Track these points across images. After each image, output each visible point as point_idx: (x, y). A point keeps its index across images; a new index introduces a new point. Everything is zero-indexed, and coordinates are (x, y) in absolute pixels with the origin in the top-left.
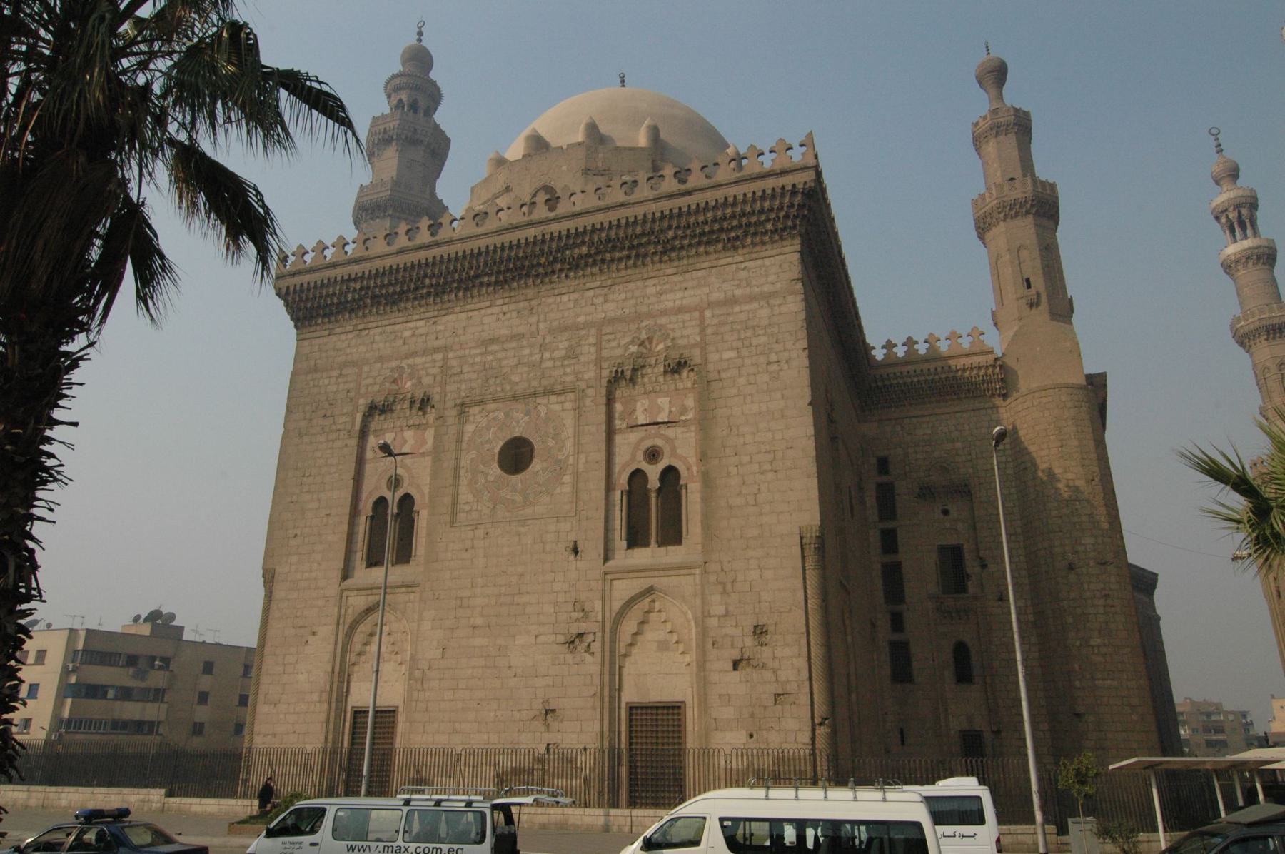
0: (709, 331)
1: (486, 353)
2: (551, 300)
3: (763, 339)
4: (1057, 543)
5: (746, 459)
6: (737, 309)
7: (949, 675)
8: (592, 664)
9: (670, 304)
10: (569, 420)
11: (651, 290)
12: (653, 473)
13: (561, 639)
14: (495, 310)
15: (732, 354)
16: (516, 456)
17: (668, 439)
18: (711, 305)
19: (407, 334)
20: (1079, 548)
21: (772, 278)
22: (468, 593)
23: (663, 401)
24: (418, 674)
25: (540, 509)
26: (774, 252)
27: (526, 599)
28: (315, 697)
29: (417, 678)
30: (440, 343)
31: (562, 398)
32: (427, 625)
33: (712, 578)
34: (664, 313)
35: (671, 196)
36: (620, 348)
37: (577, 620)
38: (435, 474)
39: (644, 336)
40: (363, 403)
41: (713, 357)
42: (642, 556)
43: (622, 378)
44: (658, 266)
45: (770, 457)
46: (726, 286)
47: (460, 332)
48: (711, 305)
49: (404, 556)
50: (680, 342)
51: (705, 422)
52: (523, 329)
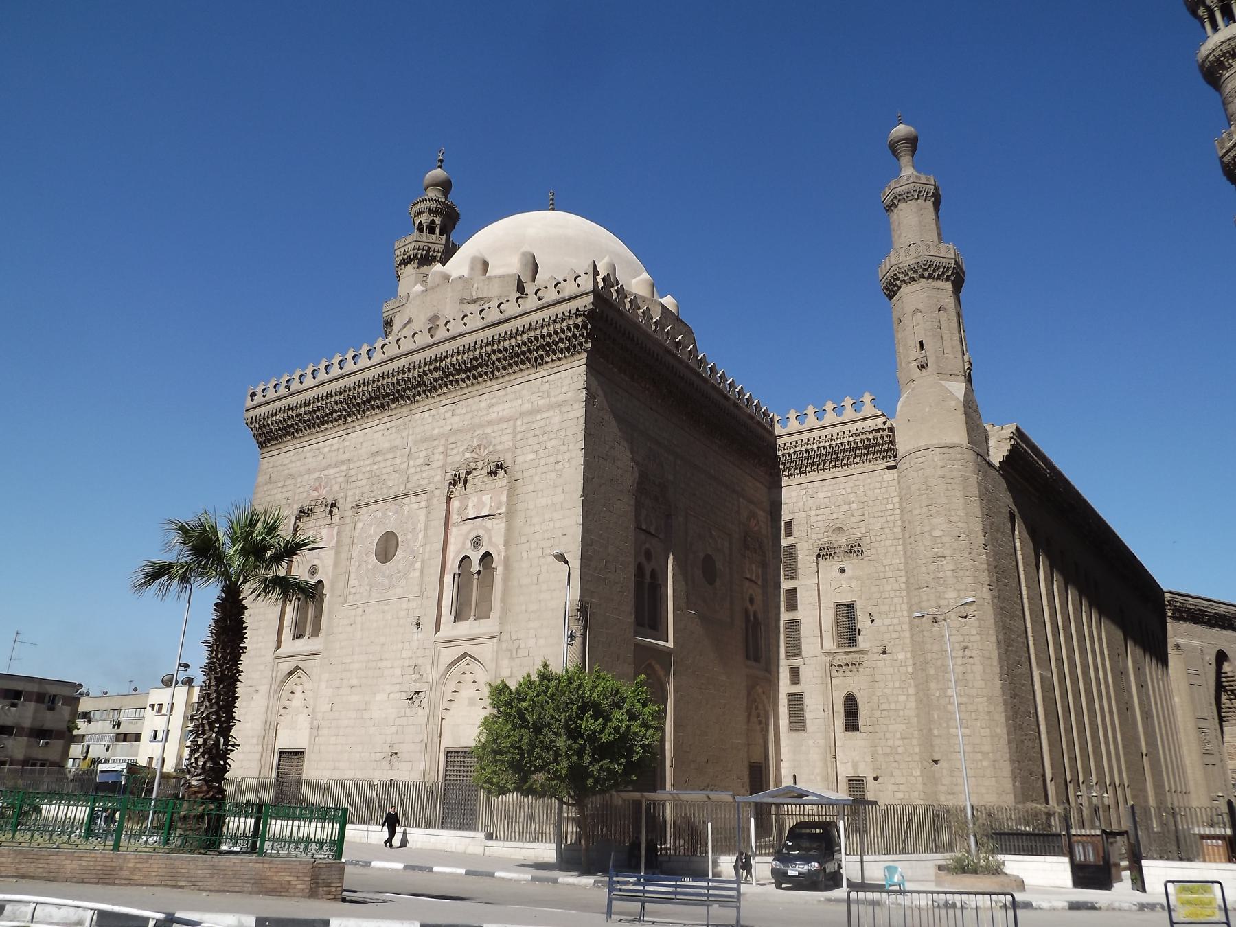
0: (519, 437)
1: (374, 463)
2: (417, 416)
3: (554, 442)
4: (925, 598)
5: (534, 545)
6: (539, 417)
7: (840, 723)
9: (495, 415)
10: (422, 518)
11: (483, 404)
12: (475, 557)
13: (404, 696)
14: (382, 427)
15: (531, 456)
16: (387, 547)
17: (488, 531)
18: (522, 414)
19: (326, 450)
20: (943, 602)
21: (565, 389)
22: (348, 660)
23: (487, 498)
24: (316, 723)
25: (399, 591)
26: (568, 366)
27: (384, 664)
28: (255, 741)
29: (315, 728)
30: (345, 457)
31: (419, 499)
32: (323, 685)
33: (504, 646)
34: (490, 423)
35: (494, 325)
36: (460, 456)
37: (415, 681)
38: (336, 565)
39: (475, 444)
40: (296, 507)
41: (520, 459)
42: (464, 628)
43: (459, 480)
44: (489, 383)
45: (550, 543)
46: (533, 398)
47: (359, 446)
48: (522, 414)
49: (316, 632)
50: (499, 448)
51: (510, 516)
52: (397, 442)
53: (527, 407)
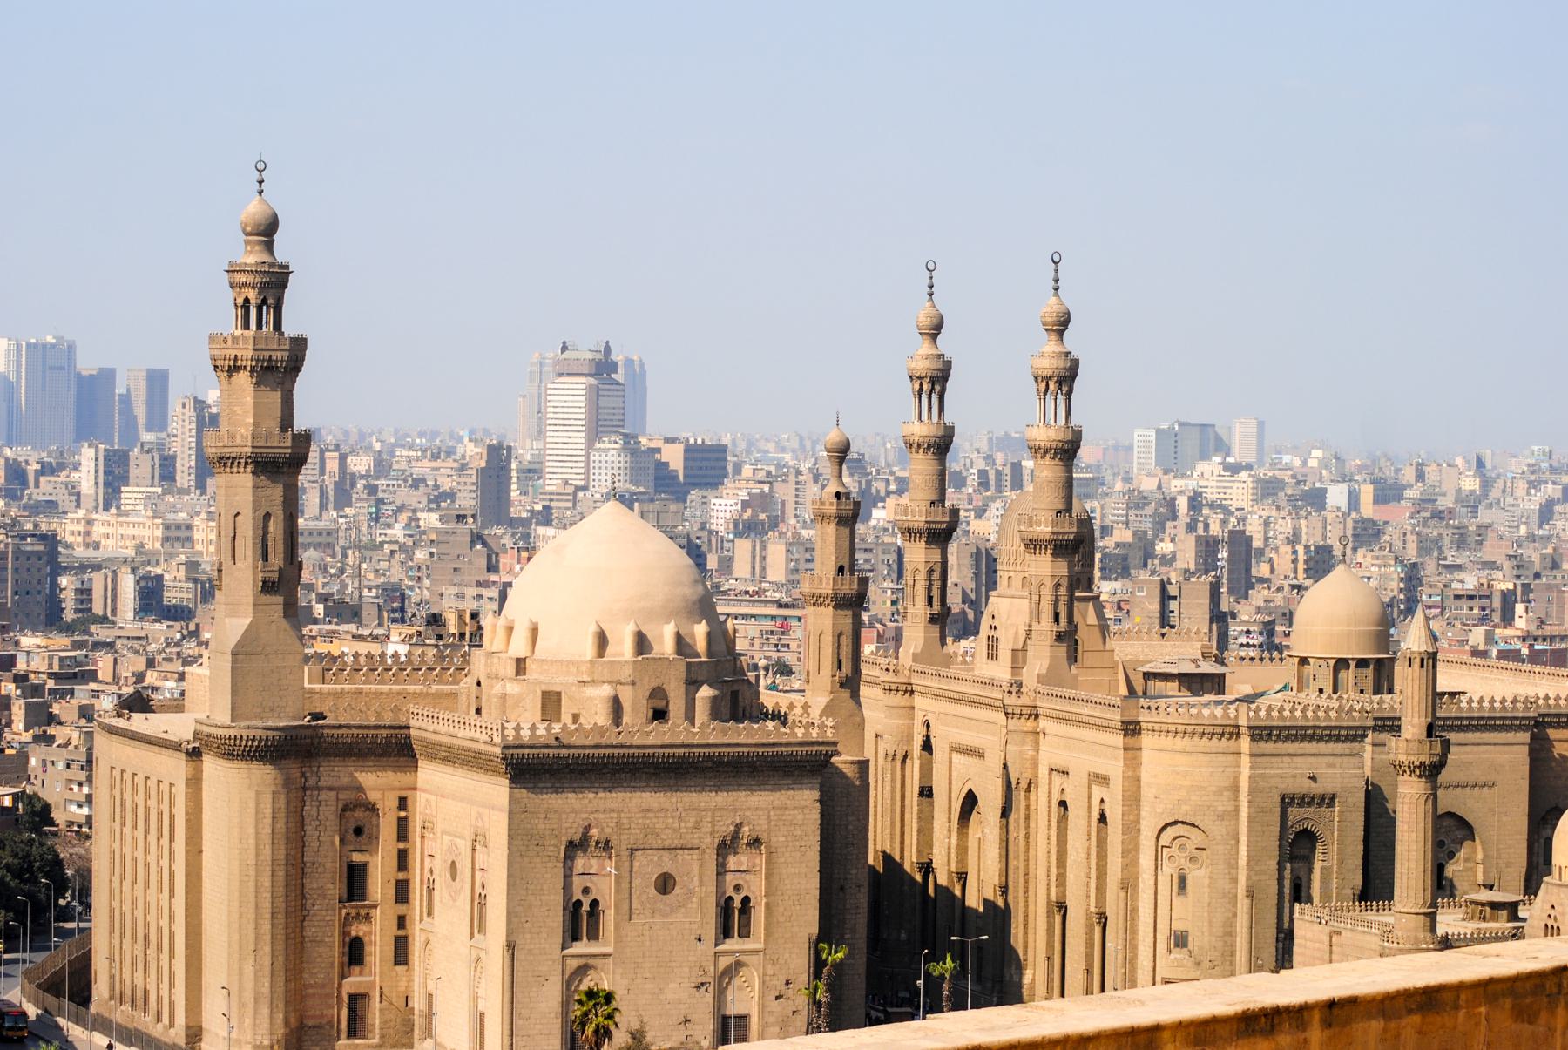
8: (709, 998)
10: (696, 867)
16: (665, 884)
30: (613, 806)
32: (618, 977)
40: (564, 840)
41: (774, 839)
49: (594, 935)
52: (667, 805)
53: (777, 803)
